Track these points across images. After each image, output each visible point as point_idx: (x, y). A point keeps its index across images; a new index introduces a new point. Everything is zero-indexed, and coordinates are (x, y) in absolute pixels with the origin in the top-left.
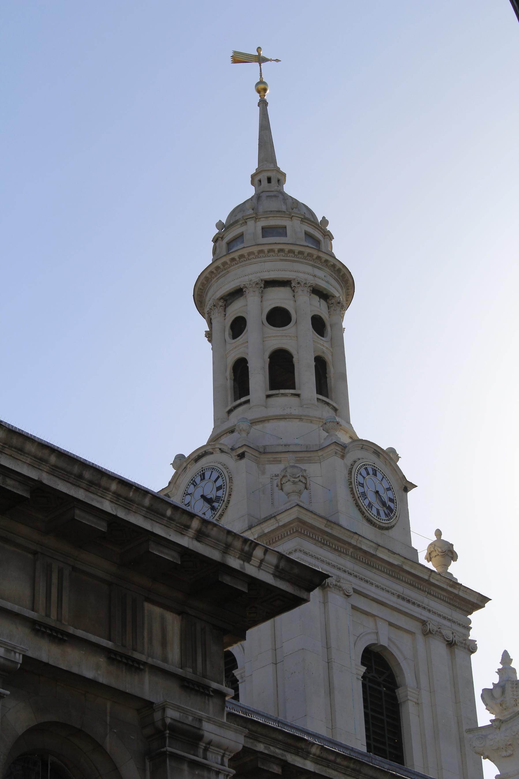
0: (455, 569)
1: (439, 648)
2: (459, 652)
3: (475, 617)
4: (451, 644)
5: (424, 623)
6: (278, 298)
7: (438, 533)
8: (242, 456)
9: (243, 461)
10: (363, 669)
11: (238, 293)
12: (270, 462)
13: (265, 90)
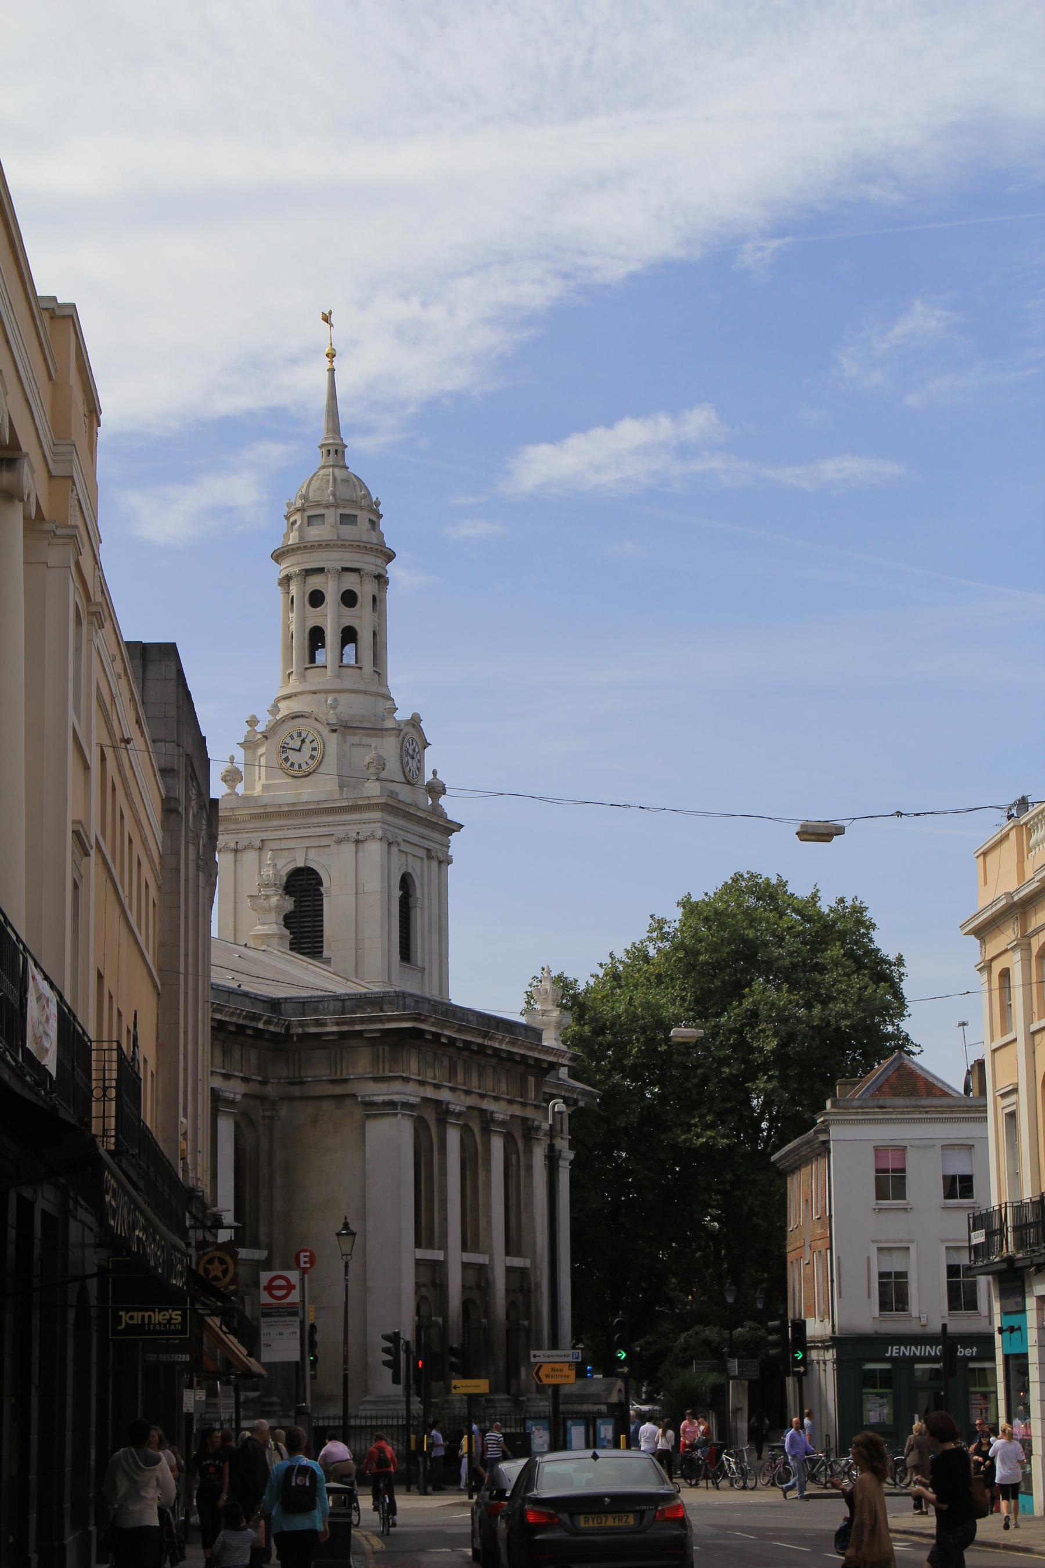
0: (443, 801)
1: (435, 864)
2: (443, 866)
3: (454, 837)
4: (440, 862)
5: (428, 850)
6: (351, 582)
7: (435, 773)
8: (334, 731)
9: (335, 735)
10: (401, 893)
11: (320, 570)
12: (350, 735)
13: (334, 356)
